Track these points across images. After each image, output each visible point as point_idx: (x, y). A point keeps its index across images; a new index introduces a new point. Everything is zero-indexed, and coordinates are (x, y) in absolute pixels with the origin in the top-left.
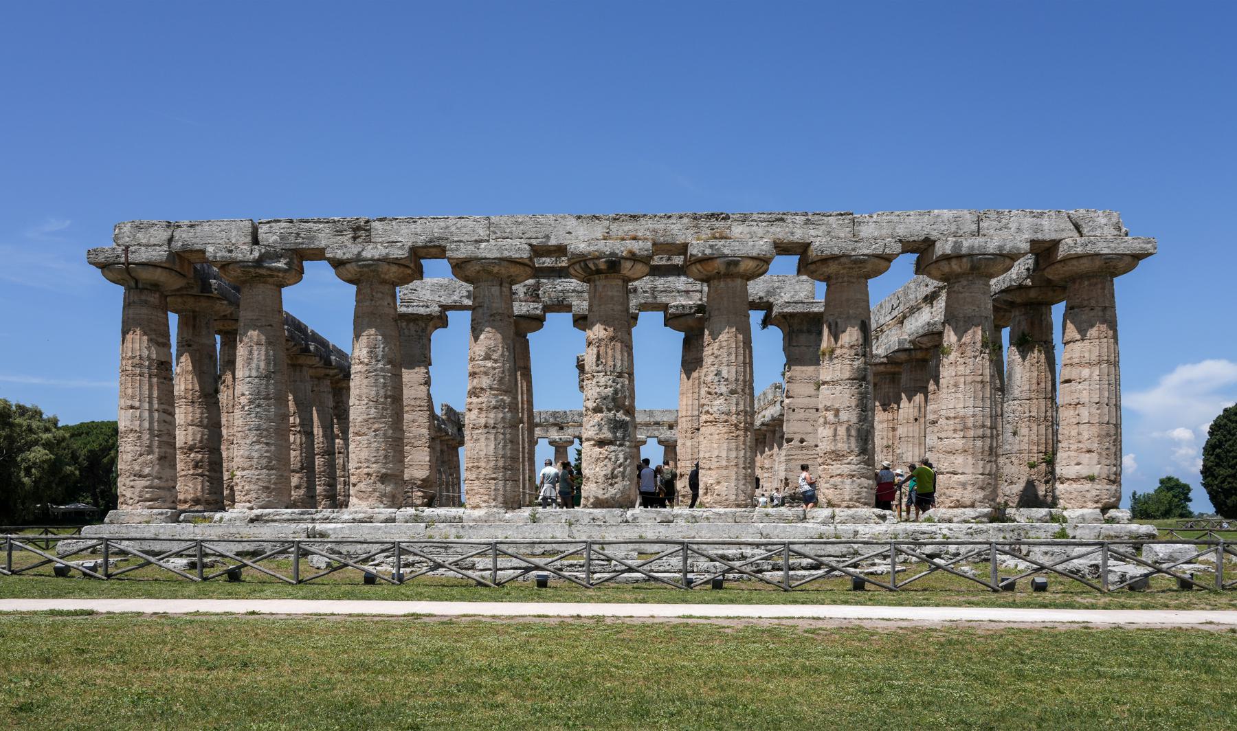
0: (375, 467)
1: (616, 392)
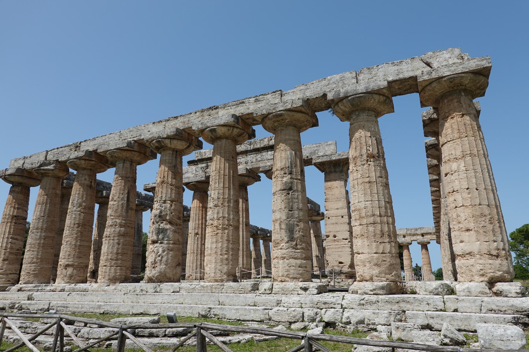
1: (161, 212)
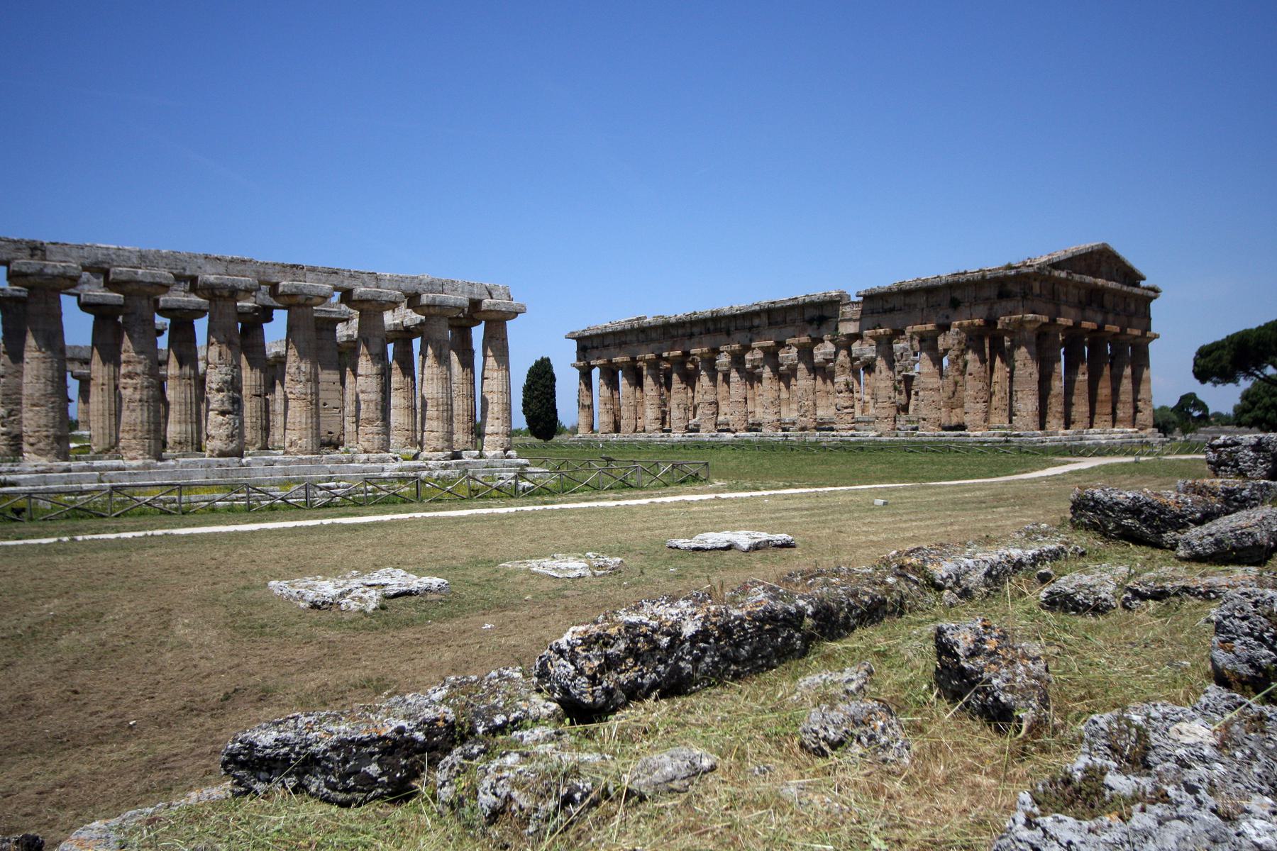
0: (52, 431)
